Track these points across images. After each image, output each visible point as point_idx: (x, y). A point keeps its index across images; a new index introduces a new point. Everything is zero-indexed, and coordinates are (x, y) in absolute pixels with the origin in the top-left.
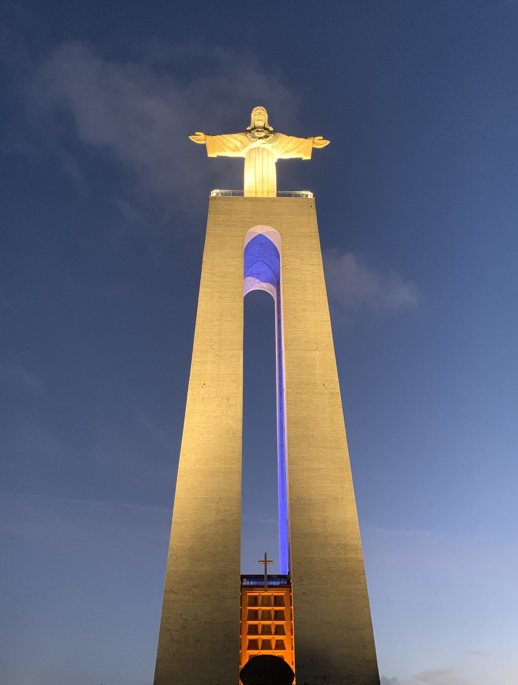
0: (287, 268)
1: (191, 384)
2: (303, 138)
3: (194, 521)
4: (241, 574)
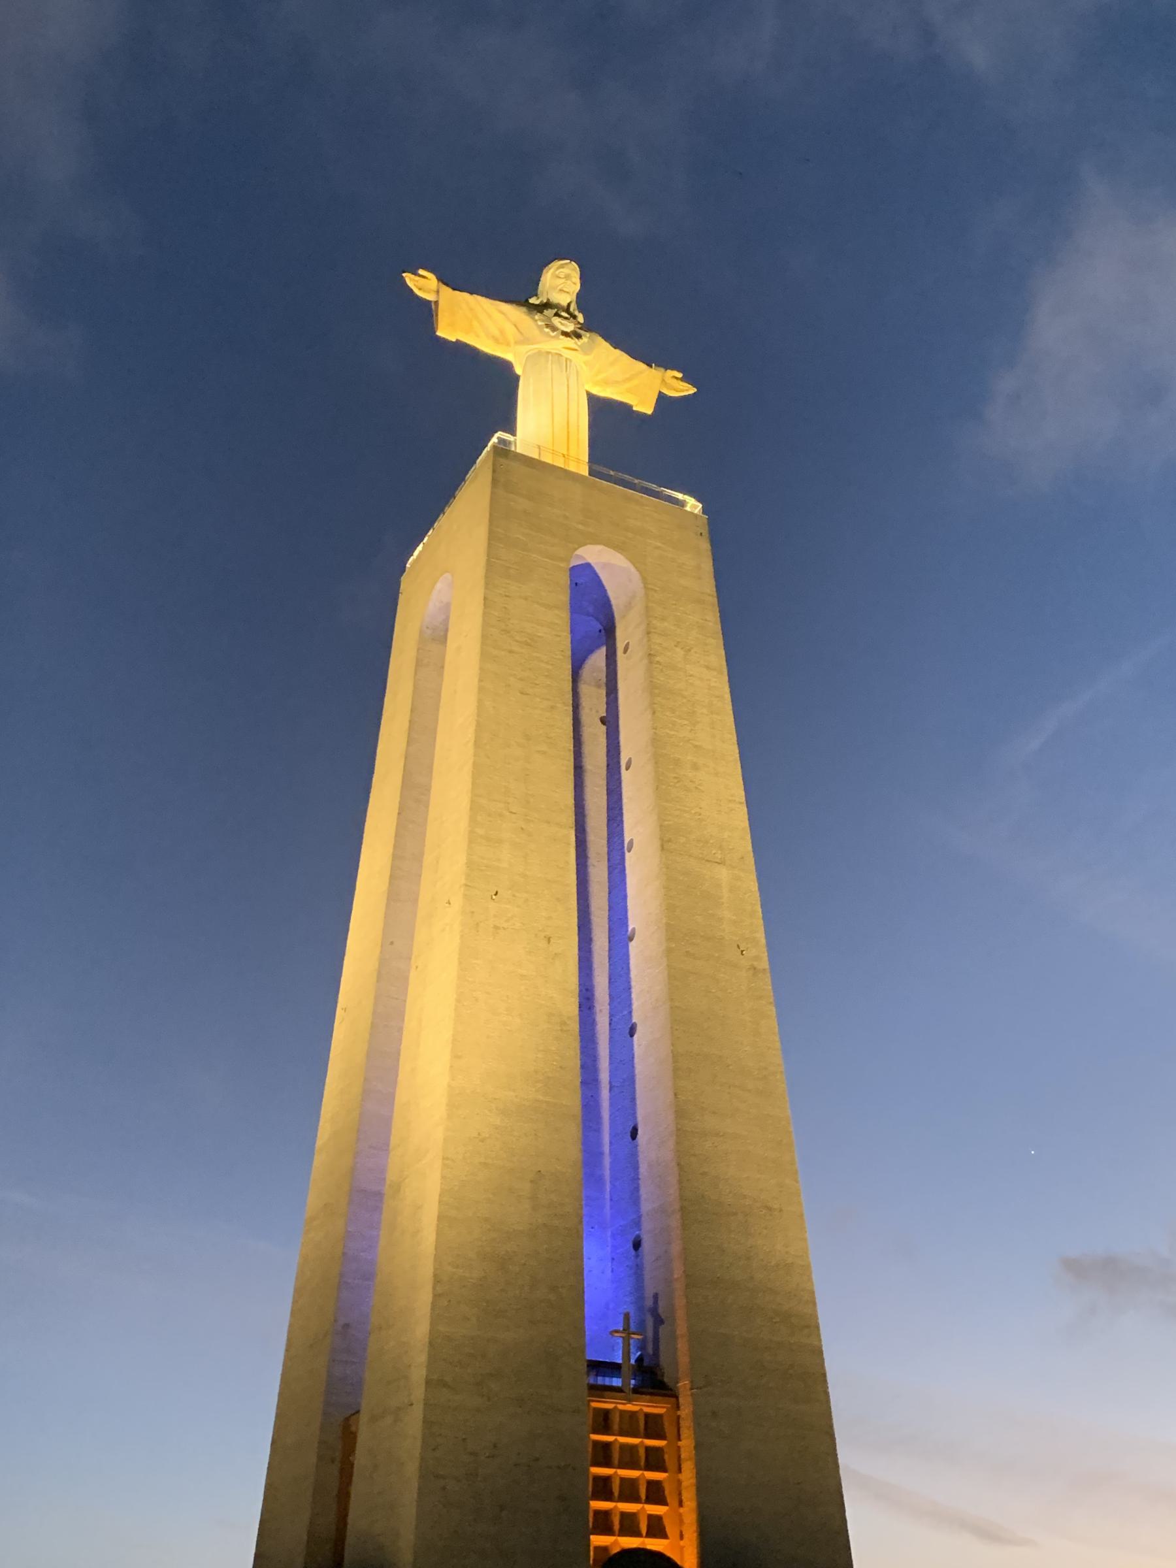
0: (658, 662)
1: (470, 886)
2: (644, 363)
4: (588, 1358)
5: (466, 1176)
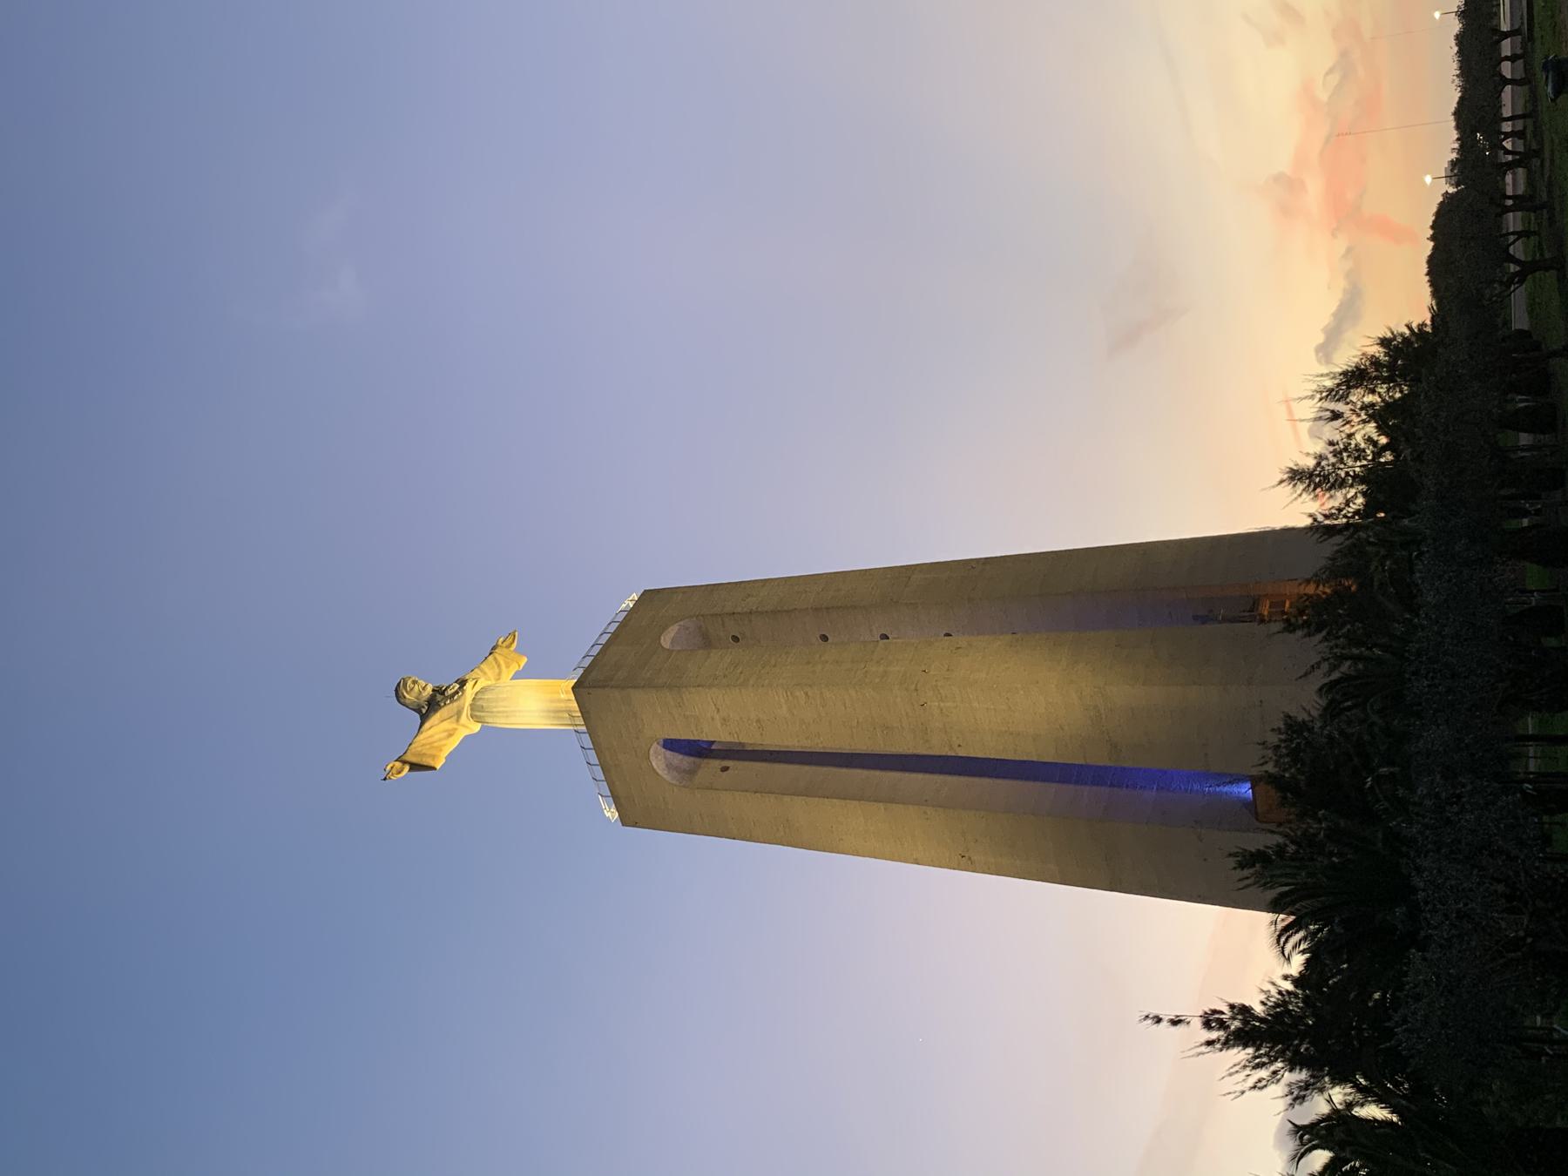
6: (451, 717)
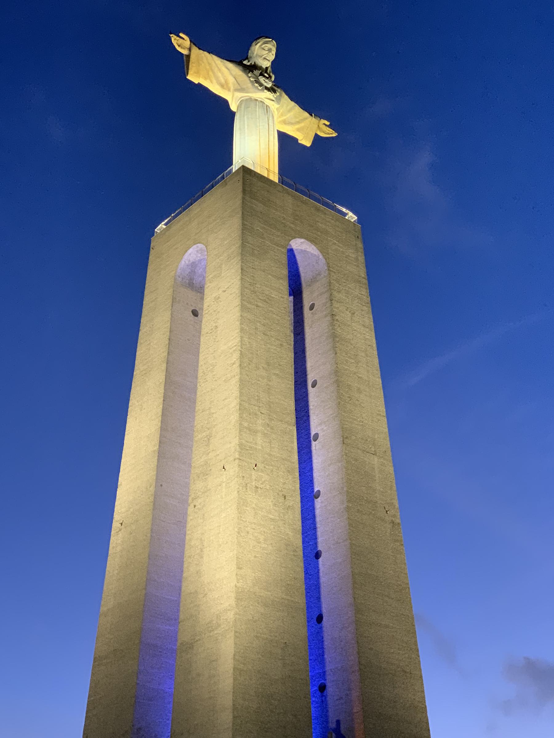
3: (259, 672)
5: (247, 644)
6: (239, 84)
